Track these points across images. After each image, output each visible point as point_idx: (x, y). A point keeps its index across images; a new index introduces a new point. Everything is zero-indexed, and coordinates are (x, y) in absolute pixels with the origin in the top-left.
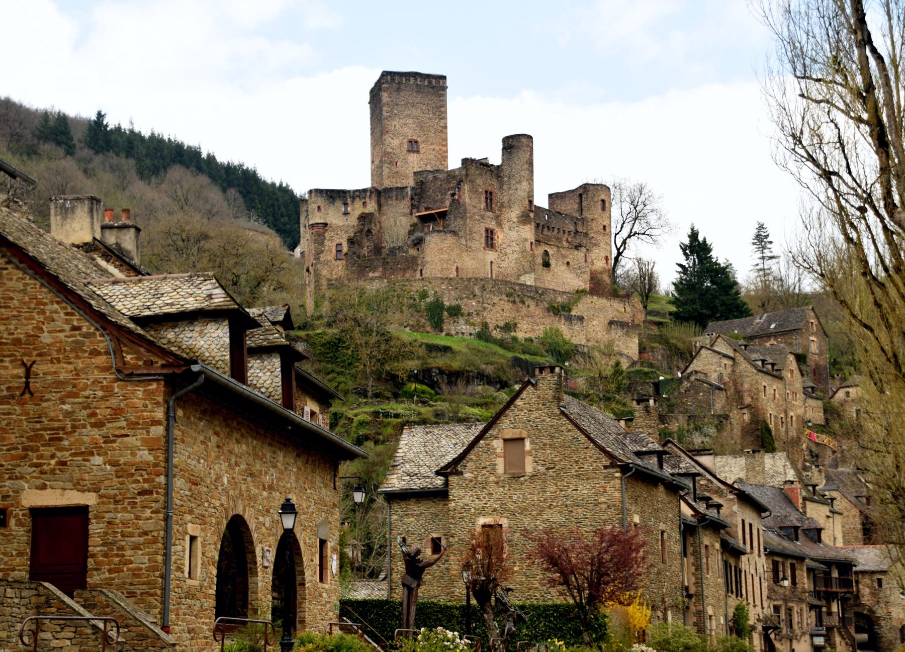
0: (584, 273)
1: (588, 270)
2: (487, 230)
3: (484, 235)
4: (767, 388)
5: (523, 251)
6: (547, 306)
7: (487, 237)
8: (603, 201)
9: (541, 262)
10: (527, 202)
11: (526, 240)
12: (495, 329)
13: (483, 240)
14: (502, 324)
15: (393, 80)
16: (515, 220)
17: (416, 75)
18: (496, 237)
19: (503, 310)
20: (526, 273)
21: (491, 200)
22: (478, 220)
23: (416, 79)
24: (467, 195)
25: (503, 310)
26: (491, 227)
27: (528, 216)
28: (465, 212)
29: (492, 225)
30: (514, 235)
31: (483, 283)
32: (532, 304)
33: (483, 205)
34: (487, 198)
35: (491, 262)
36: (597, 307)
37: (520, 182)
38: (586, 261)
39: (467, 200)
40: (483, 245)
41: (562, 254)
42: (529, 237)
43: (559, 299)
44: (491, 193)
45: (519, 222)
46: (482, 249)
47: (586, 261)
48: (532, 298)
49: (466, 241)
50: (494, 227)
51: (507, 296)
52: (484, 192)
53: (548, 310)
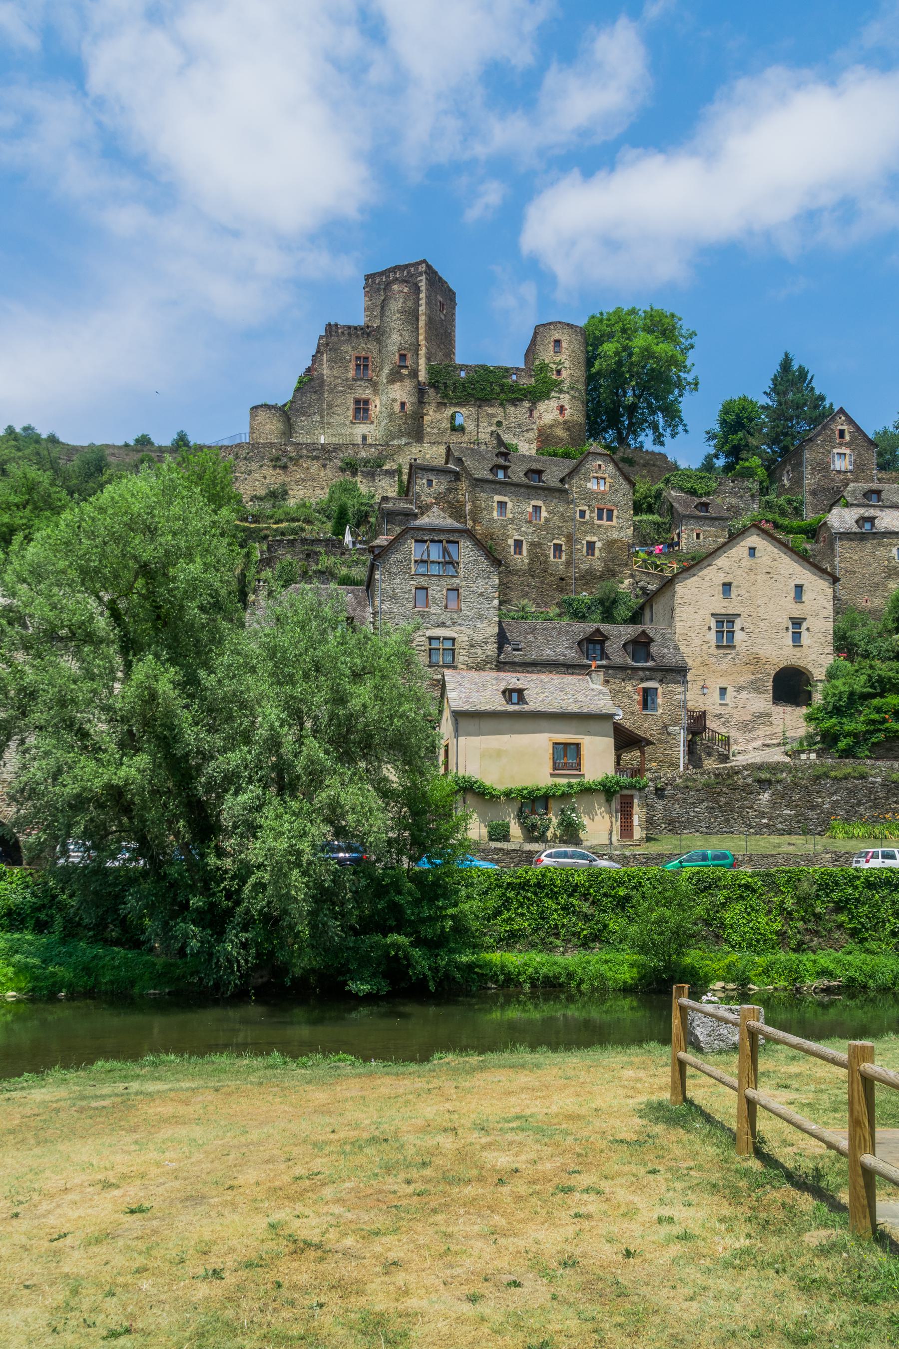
0: (528, 431)
1: (535, 427)
2: (357, 401)
3: (352, 406)
4: (510, 505)
5: (391, 416)
6: (340, 464)
7: (357, 410)
8: (558, 342)
9: (449, 425)
10: (397, 357)
11: (394, 400)
12: (251, 500)
13: (351, 413)
14: (262, 492)
15: (374, 282)
16: (385, 381)
17: (394, 269)
18: (371, 407)
19: (265, 478)
20: (393, 439)
21: (366, 366)
22: (342, 392)
23: (395, 273)
24: (324, 366)
25: (265, 478)
26: (363, 396)
27: (399, 373)
28: (322, 383)
29: (367, 394)
30: (384, 398)
31: (237, 449)
32: (315, 466)
33: (351, 374)
34: (358, 366)
35: (364, 438)
36: (428, 456)
37: (390, 337)
38: (531, 415)
39: (325, 372)
40: (351, 418)
41: (488, 414)
42: (398, 397)
43: (363, 454)
44: (366, 358)
45: (388, 382)
46: (347, 423)
47: (531, 415)
48: (316, 458)
49: (322, 417)
50: (370, 396)
51: (272, 461)
52: (353, 358)
53: (343, 470)
